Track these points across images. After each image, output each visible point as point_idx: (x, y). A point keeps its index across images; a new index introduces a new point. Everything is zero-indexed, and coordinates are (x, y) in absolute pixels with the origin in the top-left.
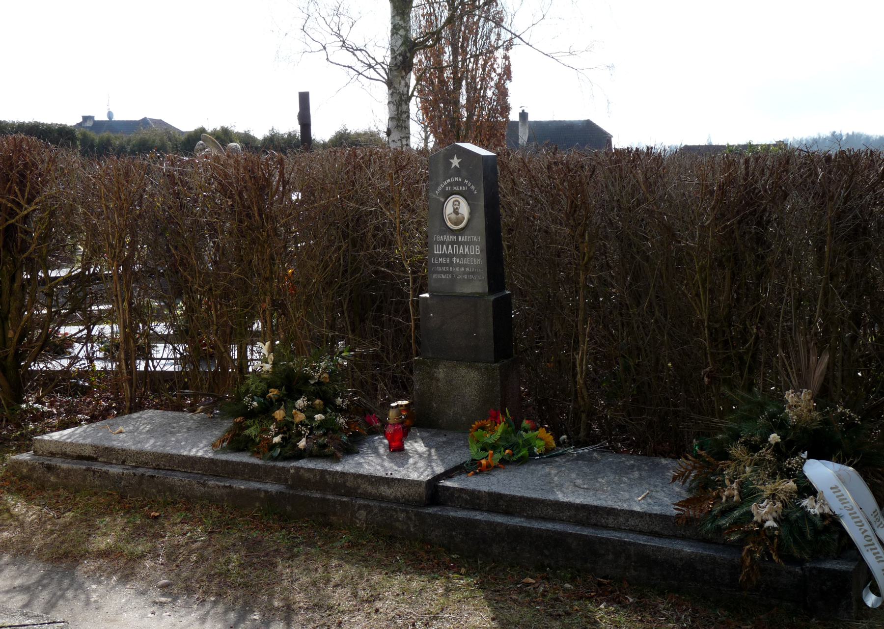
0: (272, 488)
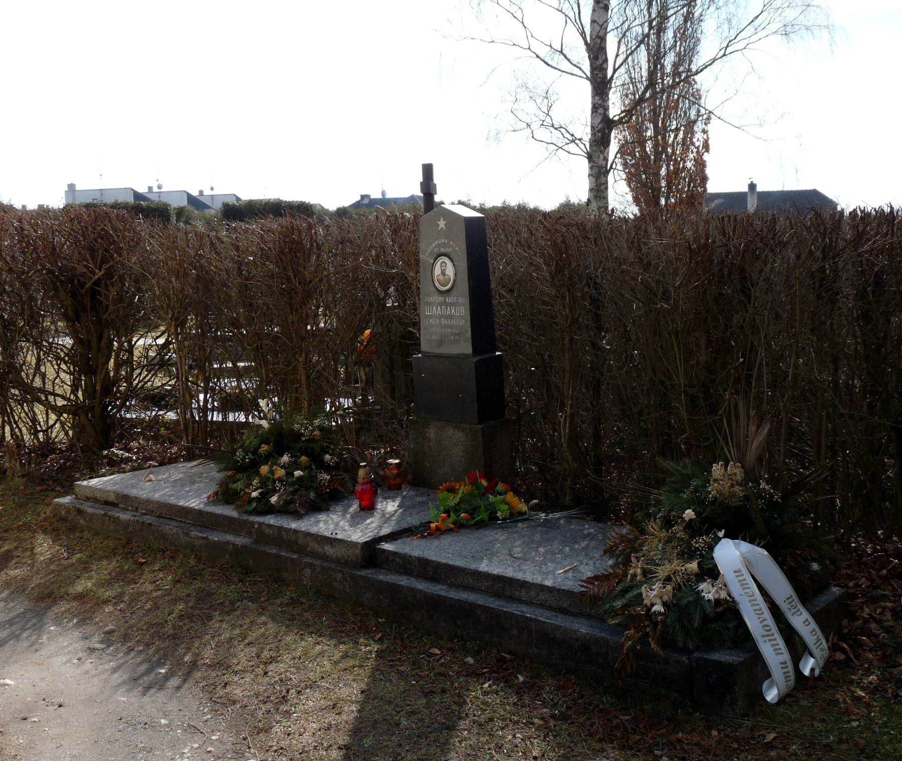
0: (240, 541)
